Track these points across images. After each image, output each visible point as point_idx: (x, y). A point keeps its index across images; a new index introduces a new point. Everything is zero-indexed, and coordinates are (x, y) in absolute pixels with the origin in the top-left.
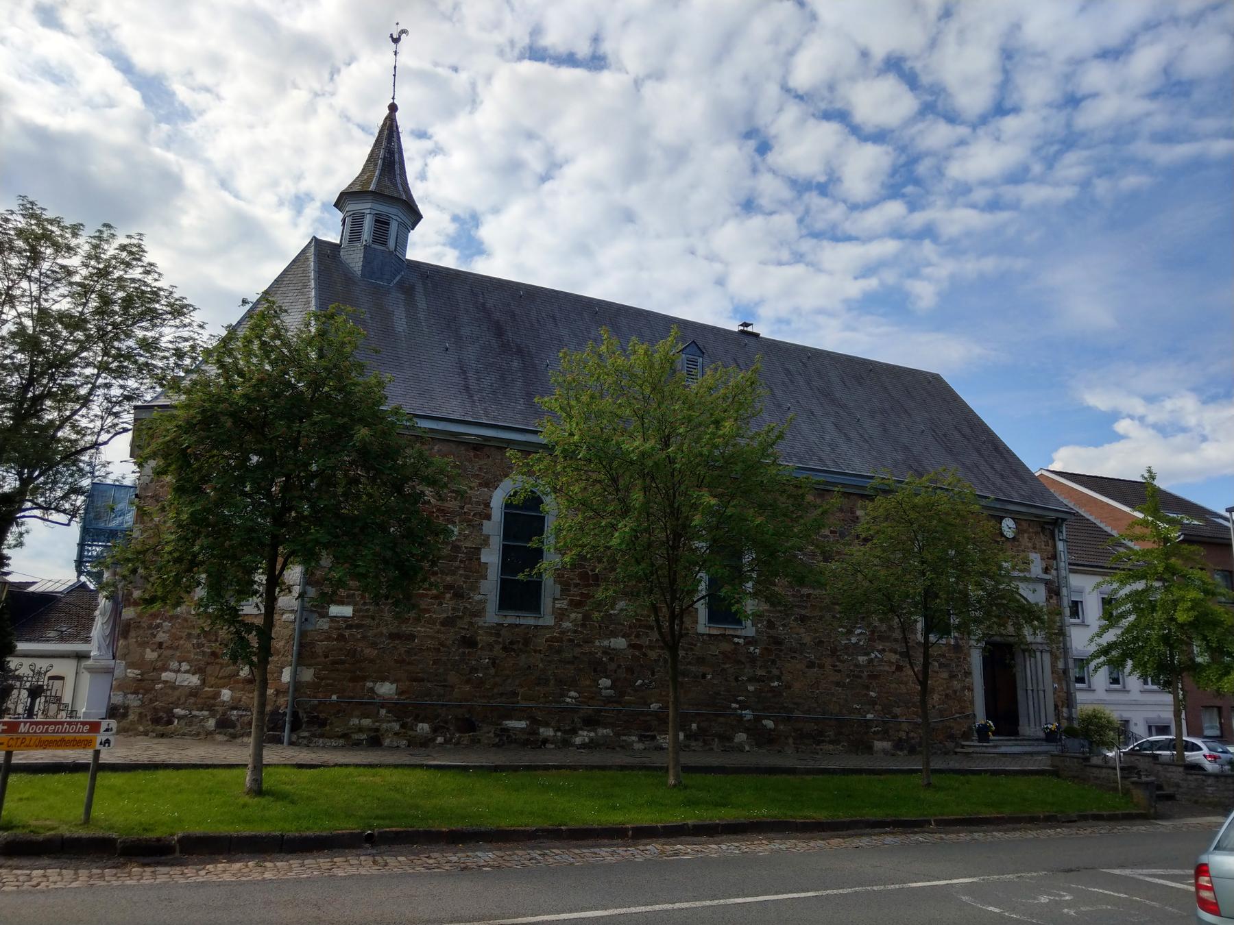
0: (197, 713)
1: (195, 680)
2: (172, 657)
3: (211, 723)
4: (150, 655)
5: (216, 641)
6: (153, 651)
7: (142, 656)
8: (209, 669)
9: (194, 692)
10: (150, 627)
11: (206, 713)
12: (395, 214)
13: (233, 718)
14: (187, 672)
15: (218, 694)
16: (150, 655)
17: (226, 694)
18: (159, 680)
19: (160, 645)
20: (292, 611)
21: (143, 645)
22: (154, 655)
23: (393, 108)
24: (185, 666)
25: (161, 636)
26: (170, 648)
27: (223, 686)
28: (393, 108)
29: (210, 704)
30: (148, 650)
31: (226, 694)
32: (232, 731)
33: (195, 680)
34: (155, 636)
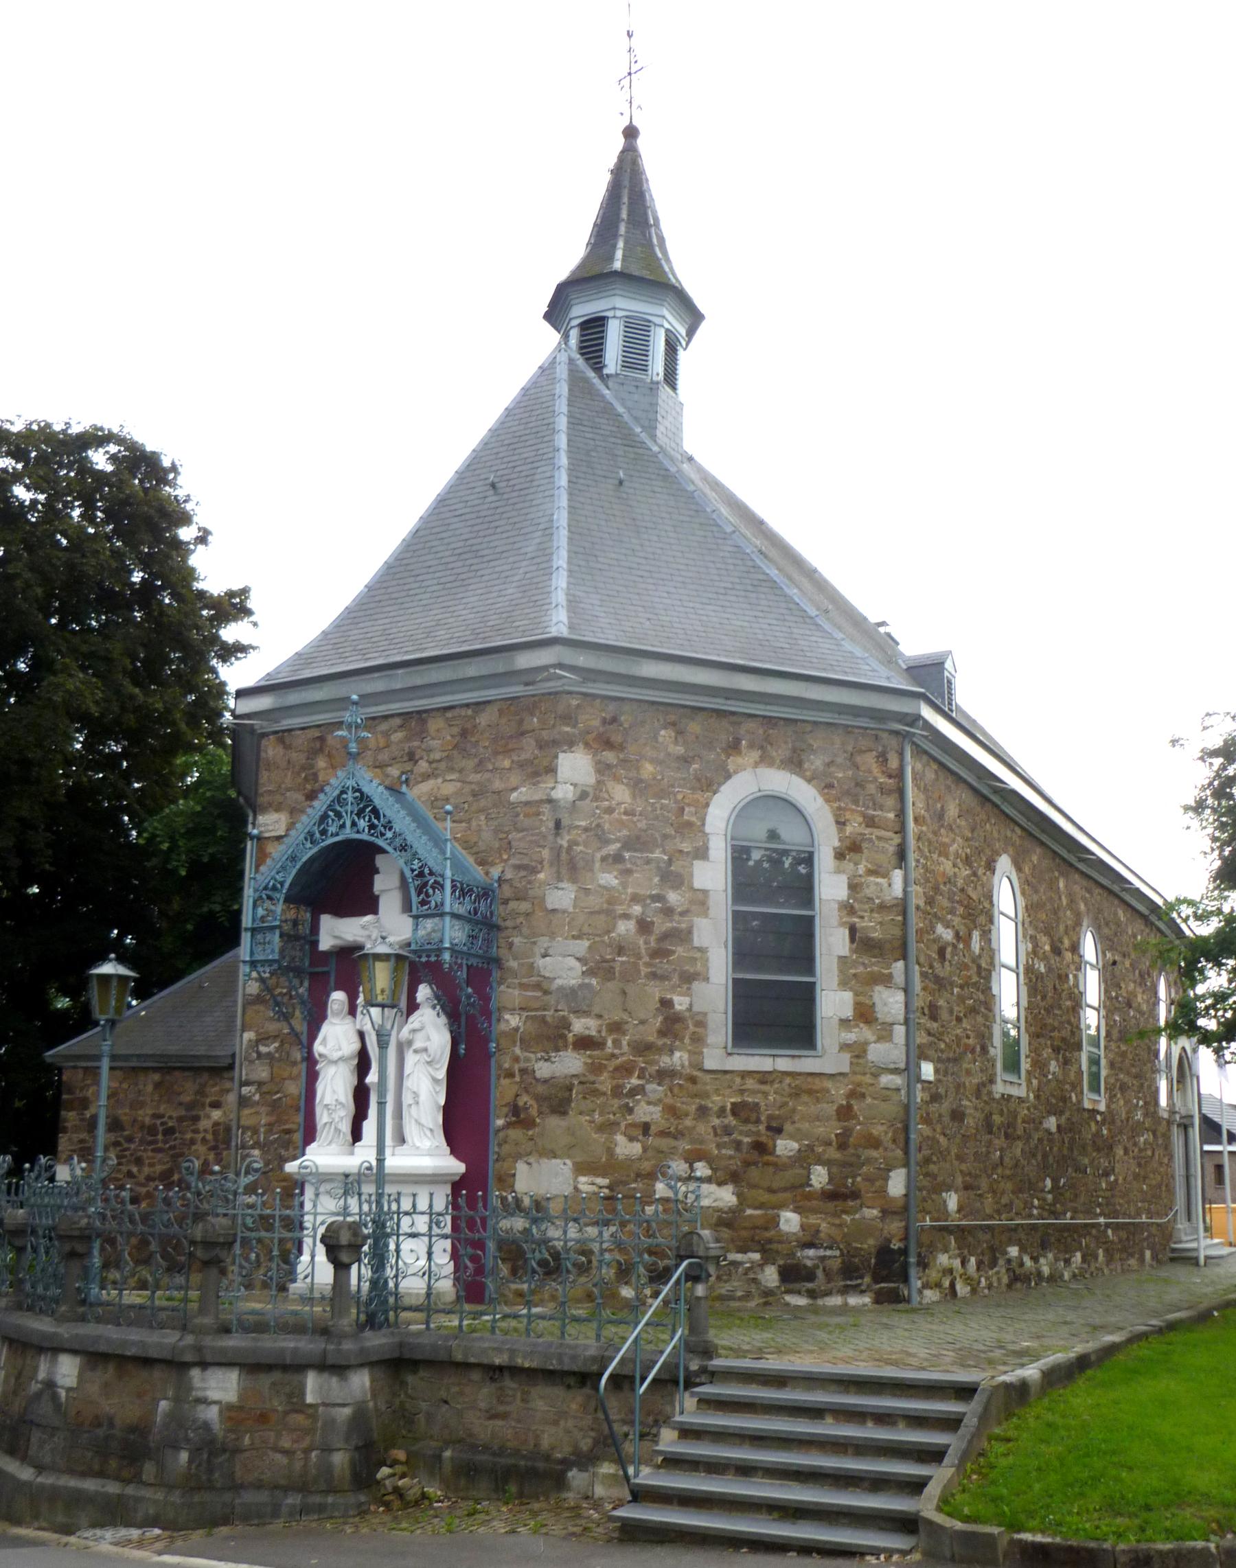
0: (739, 1257)
1: (725, 1196)
2: (673, 1152)
3: (770, 1276)
4: (626, 1148)
5: (758, 1121)
6: (632, 1139)
7: (610, 1152)
8: (754, 1174)
9: (725, 1221)
10: (617, 1092)
11: (756, 1256)
12: (668, 319)
13: (809, 1263)
14: (709, 1180)
15: (775, 1221)
16: (626, 1148)
17: (790, 1221)
18: (648, 1198)
19: (646, 1128)
20: (895, 1071)
21: (609, 1127)
22: (636, 1149)
23: (631, 133)
24: (702, 1169)
25: (646, 1112)
26: (663, 1134)
27: (782, 1206)
28: (631, 133)
29: (762, 1239)
30: (620, 1138)
31: (790, 1221)
32: (810, 1285)
33: (725, 1196)
34: (630, 1111)
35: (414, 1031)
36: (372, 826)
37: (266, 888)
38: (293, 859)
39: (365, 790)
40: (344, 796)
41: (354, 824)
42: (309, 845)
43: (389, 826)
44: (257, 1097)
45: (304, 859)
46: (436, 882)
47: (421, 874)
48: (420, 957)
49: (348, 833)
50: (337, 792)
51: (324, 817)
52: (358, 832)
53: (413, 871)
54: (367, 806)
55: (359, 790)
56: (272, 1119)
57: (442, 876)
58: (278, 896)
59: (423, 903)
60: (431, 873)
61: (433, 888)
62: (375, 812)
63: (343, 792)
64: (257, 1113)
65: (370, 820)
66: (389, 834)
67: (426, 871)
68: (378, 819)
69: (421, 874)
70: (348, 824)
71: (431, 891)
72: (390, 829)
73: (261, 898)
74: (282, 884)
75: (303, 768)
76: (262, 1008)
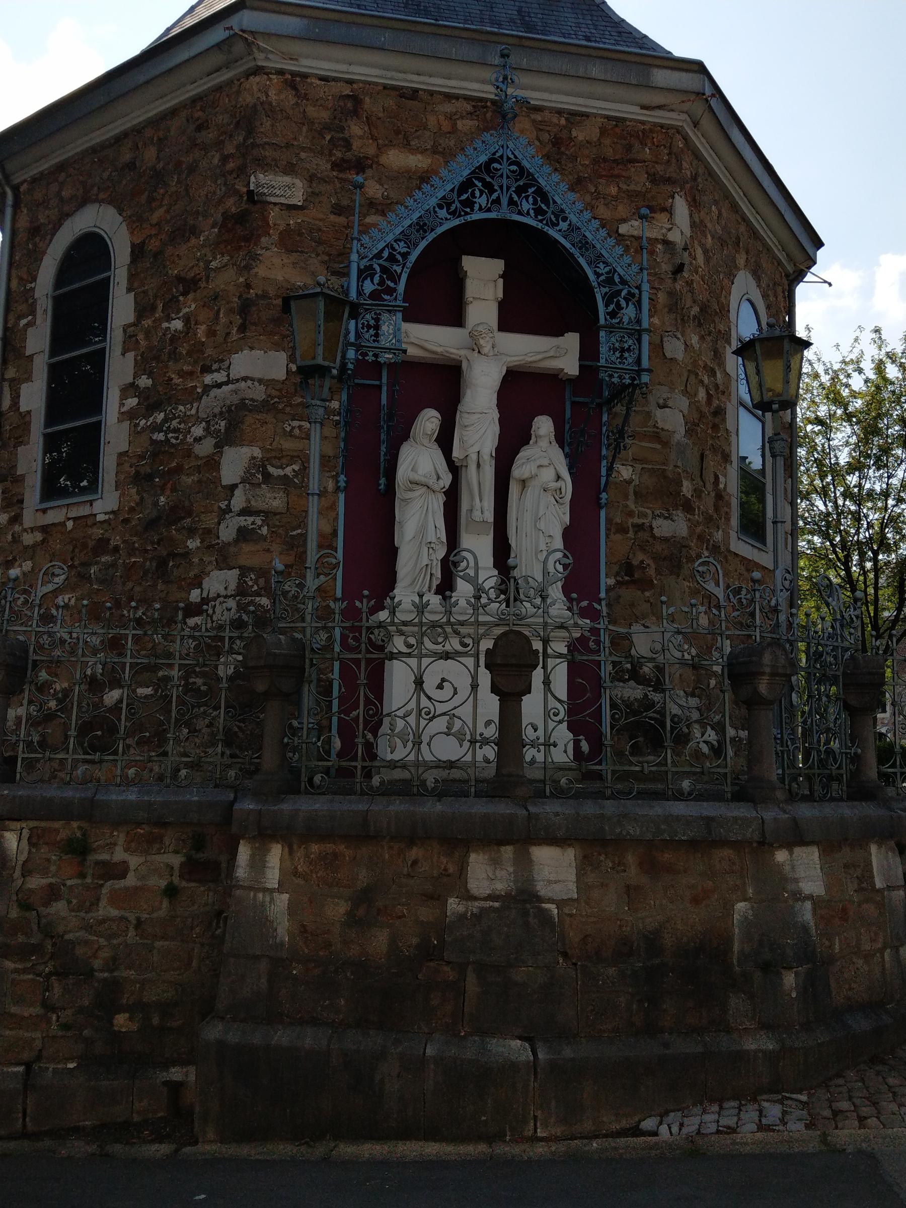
35: (540, 466)
36: (539, 212)
37: (378, 256)
38: (421, 227)
39: (525, 163)
40: (496, 165)
41: (511, 202)
42: (443, 213)
43: (561, 215)
44: (265, 531)
45: (440, 230)
46: (629, 293)
47: (609, 281)
48: (611, 376)
49: (504, 213)
50: (483, 158)
51: (466, 185)
52: (520, 213)
53: (598, 275)
54: (532, 186)
55: (517, 163)
56: (290, 559)
57: (639, 287)
58: (399, 269)
59: (613, 315)
60: (623, 282)
61: (627, 300)
62: (541, 194)
63: (492, 160)
64: (268, 550)
65: (535, 202)
66: (564, 226)
67: (617, 279)
68: (548, 206)
69: (609, 281)
70: (505, 201)
71: (623, 303)
72: (565, 219)
73: (370, 267)
74: (405, 255)
75: (327, 127)
76: (269, 418)
